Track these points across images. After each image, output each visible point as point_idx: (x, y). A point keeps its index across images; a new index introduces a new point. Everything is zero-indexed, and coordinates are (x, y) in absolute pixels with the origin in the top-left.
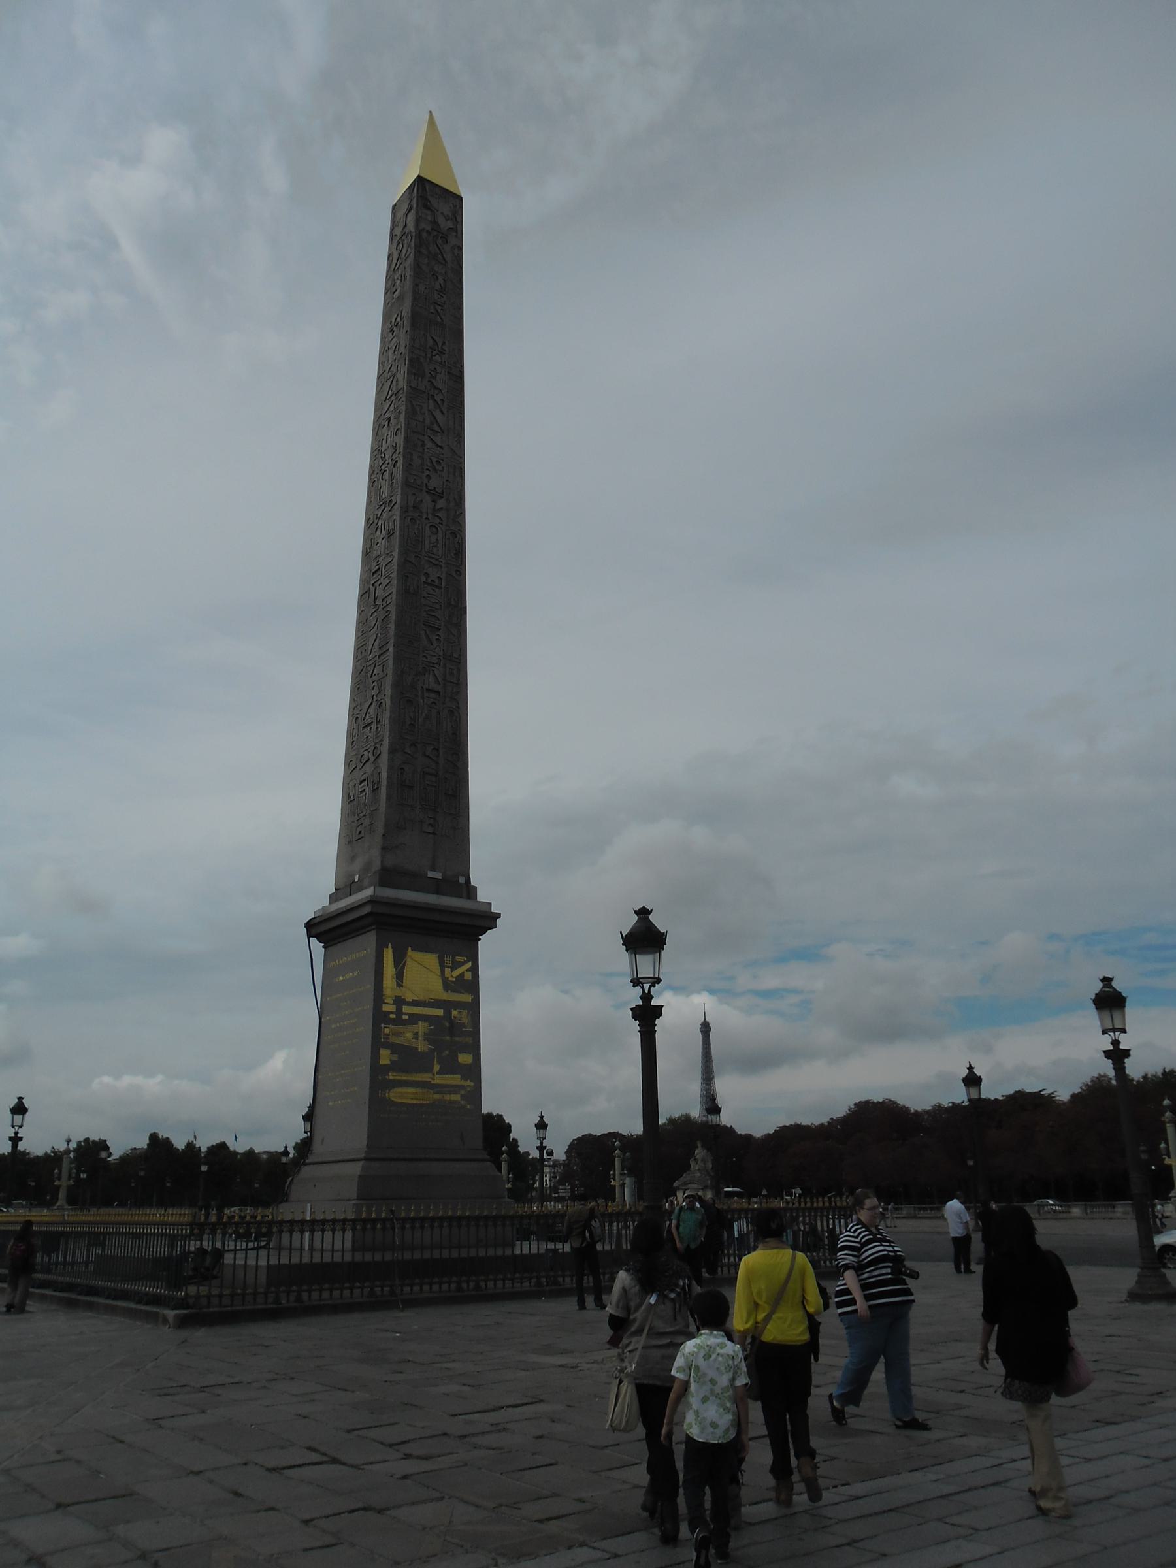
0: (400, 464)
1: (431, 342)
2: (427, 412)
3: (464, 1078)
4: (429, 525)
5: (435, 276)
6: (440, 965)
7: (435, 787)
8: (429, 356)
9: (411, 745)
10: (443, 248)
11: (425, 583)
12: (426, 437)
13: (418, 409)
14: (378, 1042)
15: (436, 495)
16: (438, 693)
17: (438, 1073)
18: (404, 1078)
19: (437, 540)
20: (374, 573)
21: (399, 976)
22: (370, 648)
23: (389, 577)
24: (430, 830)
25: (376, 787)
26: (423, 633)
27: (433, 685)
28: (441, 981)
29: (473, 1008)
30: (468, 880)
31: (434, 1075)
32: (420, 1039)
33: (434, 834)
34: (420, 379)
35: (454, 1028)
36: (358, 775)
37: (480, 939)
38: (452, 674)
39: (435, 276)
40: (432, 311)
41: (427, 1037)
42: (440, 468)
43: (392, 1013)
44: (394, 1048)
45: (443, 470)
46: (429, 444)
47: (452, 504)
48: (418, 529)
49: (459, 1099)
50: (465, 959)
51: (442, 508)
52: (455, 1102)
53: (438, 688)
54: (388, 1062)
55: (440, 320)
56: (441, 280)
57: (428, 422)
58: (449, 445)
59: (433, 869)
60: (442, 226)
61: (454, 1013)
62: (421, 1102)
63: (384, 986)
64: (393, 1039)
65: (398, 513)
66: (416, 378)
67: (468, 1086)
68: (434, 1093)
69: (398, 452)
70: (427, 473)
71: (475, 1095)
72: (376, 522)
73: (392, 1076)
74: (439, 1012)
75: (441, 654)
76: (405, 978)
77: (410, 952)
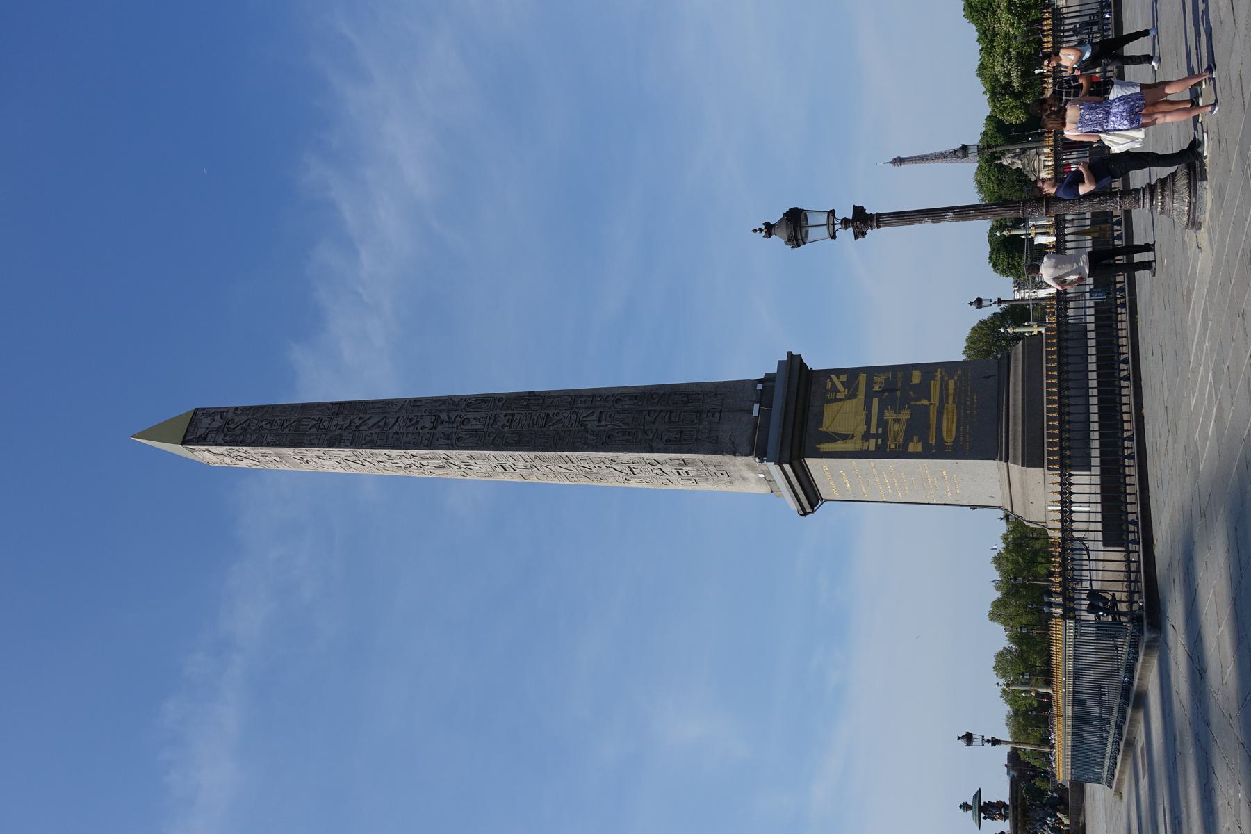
0: (414, 452)
1: (314, 430)
2: (370, 431)
3: (934, 378)
4: (462, 427)
5: (260, 428)
6: (835, 402)
7: (681, 412)
9: (646, 433)
10: (237, 423)
12: (390, 431)
13: (368, 439)
14: (902, 454)
15: (437, 421)
16: (601, 412)
17: (930, 401)
18: (934, 430)
20: (505, 470)
21: (845, 437)
22: (567, 471)
23: (506, 458)
24: (717, 415)
25: (682, 462)
26: (551, 427)
27: (595, 418)
28: (848, 401)
29: (872, 372)
30: (760, 381)
31: (931, 404)
32: (899, 418)
33: (721, 412)
34: (344, 438)
35: (889, 388)
36: (674, 477)
37: (811, 368)
38: (585, 402)
39: (260, 428)
40: (288, 429)
41: (897, 411)
42: (415, 418)
43: (877, 442)
44: (907, 439)
45: (417, 416)
46: (396, 428)
47: (444, 407)
48: (466, 435)
49: (953, 381)
50: (828, 381)
51: (448, 416)
52: (955, 384)
53: (597, 413)
54: (921, 443)
55: (295, 424)
56: (264, 423)
57: (378, 430)
58: (396, 412)
59: (751, 411)
61: (876, 388)
62: (955, 414)
63: (853, 450)
64: (900, 440)
65: (454, 452)
66: (343, 441)
67: (941, 374)
68: (948, 403)
69: (404, 454)
70: (419, 430)
71: (949, 367)
72: (464, 470)
73: (932, 441)
74: (876, 401)
75: (568, 412)
76: (845, 433)
77: (824, 429)
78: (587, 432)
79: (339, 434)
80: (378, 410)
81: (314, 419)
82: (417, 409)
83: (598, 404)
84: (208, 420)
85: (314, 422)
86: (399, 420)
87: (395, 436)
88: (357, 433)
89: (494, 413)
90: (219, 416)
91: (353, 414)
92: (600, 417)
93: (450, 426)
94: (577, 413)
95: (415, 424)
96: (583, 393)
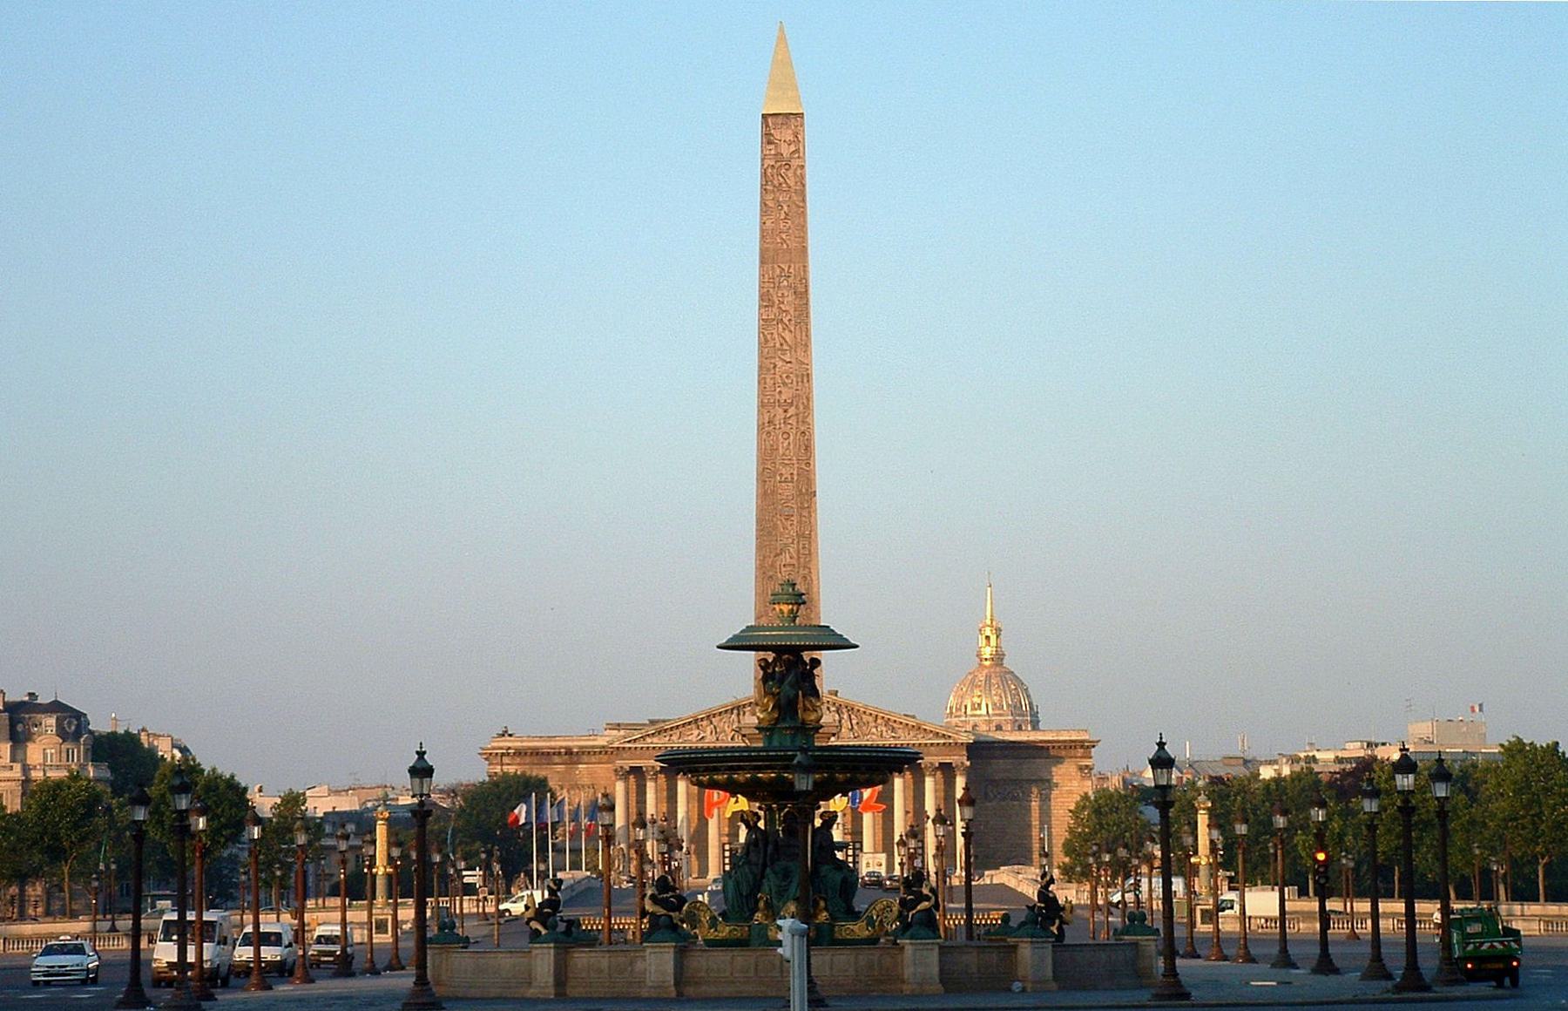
1: (778, 271)
8: (777, 285)
11: (780, 482)
12: (777, 359)
13: (769, 337)
19: (789, 443)
26: (779, 522)
40: (779, 241)
45: (792, 383)
46: (780, 364)
47: (801, 407)
55: (785, 246)
56: (786, 208)
57: (778, 345)
60: (784, 155)
70: (778, 390)
75: (795, 534)
78: (775, 557)
79: (774, 303)
80: (799, 337)
81: (789, 267)
82: (800, 380)
83: (802, 560)
84: (789, 136)
85: (786, 269)
86: (789, 365)
87: (772, 366)
88: (775, 323)
89: (795, 462)
90: (794, 149)
91: (795, 311)
92: (790, 565)
93: (782, 421)
94: (793, 543)
95: (785, 384)
96: (813, 545)
